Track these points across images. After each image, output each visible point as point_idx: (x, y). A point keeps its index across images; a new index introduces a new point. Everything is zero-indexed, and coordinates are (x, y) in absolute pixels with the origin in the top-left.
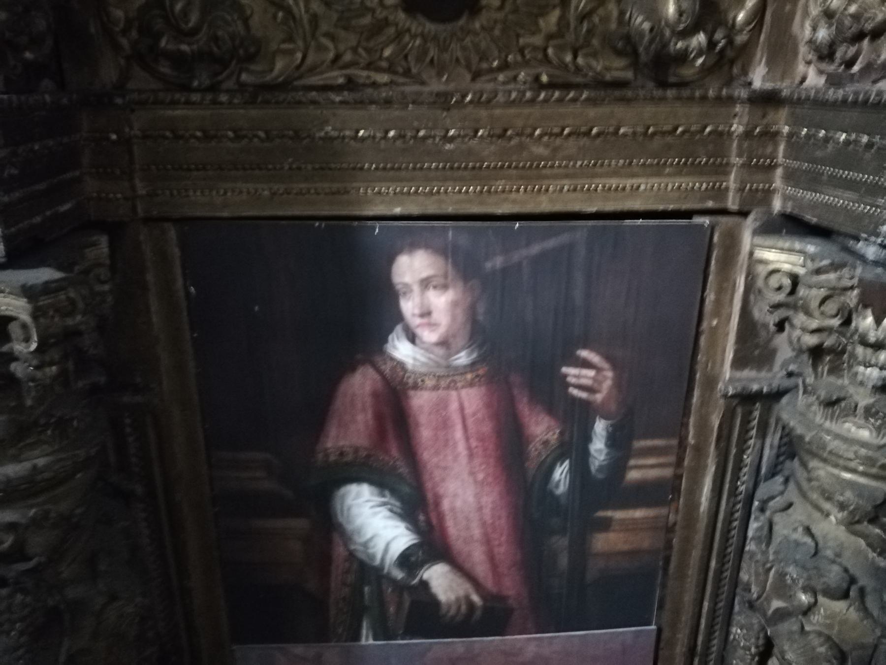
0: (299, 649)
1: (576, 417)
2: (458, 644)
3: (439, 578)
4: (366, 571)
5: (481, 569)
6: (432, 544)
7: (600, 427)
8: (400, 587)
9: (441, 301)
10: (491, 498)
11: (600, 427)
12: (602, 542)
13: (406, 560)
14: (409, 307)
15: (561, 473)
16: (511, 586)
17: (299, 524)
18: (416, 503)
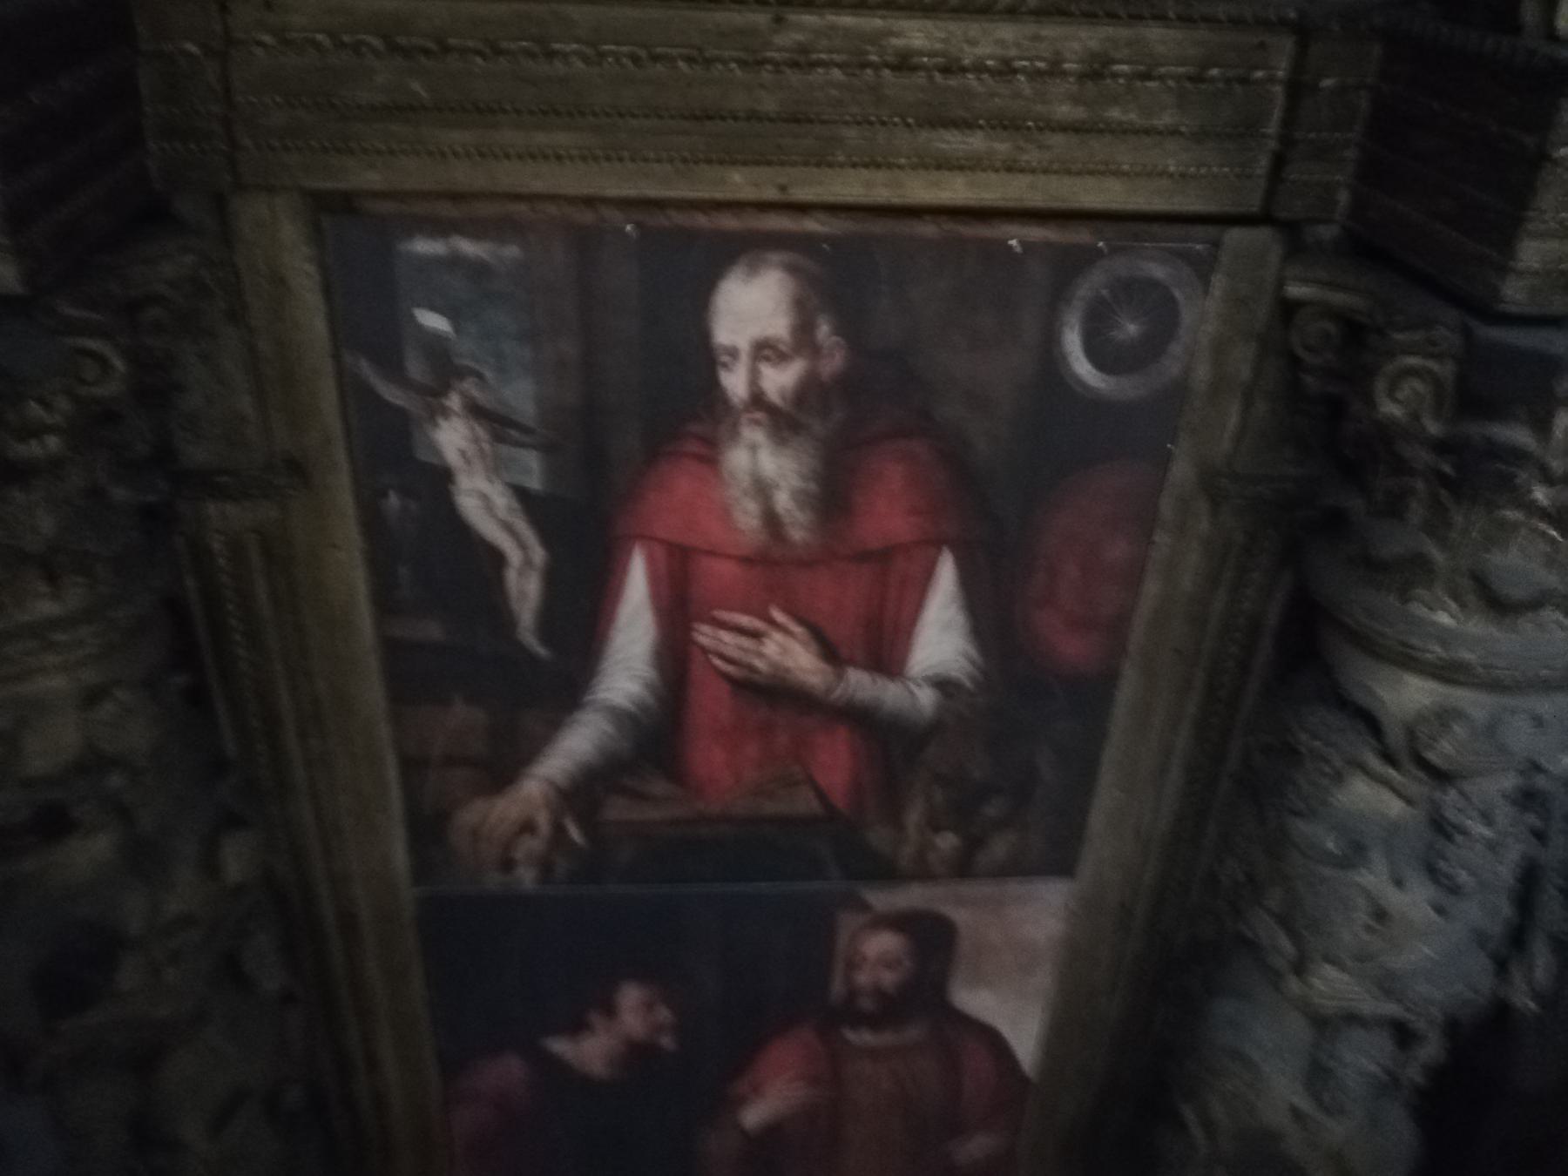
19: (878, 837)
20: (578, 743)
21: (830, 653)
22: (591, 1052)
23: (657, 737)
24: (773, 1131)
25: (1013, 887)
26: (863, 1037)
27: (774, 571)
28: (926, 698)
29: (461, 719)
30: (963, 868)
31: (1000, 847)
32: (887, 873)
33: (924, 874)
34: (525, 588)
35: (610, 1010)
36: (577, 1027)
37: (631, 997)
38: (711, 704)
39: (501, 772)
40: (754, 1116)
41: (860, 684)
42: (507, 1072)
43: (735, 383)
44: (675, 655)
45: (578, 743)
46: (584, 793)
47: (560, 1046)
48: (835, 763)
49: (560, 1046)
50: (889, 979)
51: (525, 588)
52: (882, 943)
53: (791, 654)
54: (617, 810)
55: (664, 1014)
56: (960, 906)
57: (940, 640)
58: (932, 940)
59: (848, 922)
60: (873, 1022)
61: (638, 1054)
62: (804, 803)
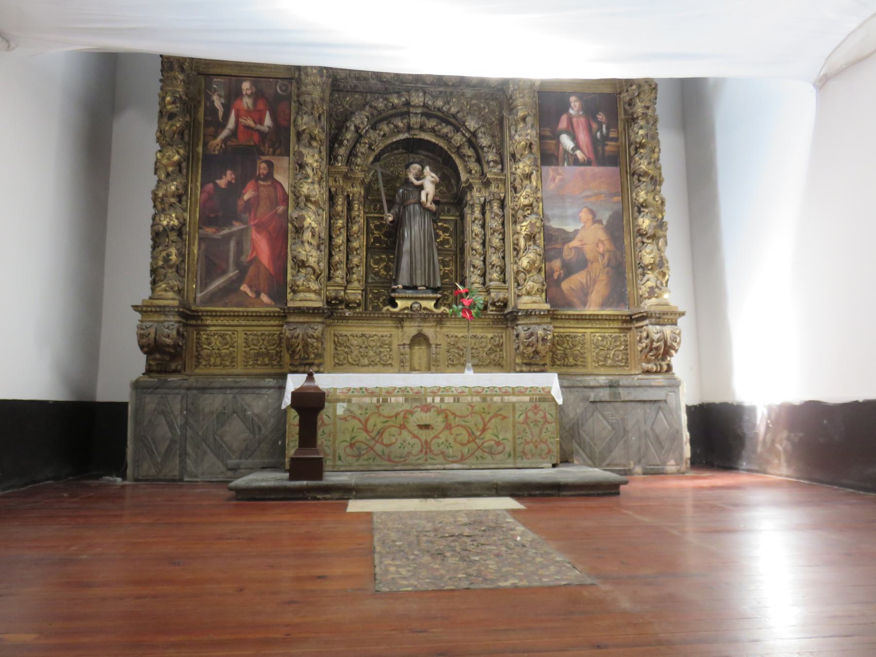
0: (553, 167)
1: (600, 124)
2: (583, 168)
3: (579, 153)
4: (566, 152)
5: (586, 152)
6: (577, 147)
7: (604, 126)
8: (572, 155)
9: (577, 104)
10: (587, 138)
11: (604, 126)
12: (607, 148)
13: (573, 149)
14: (572, 105)
15: (598, 134)
16: (592, 156)
17: (554, 142)
18: (574, 138)
19: (262, 149)
20: (225, 133)
21: (255, 123)
22: (222, 183)
23: (234, 133)
24: (249, 200)
25: (281, 158)
26: (261, 183)
27: (249, 113)
28: (267, 129)
29: (211, 130)
30: (274, 154)
31: (278, 151)
32: (263, 154)
33: (268, 154)
34: (221, 114)
35: (226, 175)
36: (221, 178)
37: (229, 172)
38: (241, 129)
39: (215, 136)
40: (246, 197)
41: (259, 127)
42: (210, 186)
43: (244, 92)
44: (237, 122)
45: (225, 133)
46: (225, 141)
47: (218, 181)
48: (256, 137)
49: (218, 181)
50: (265, 172)
51: (221, 114)
52: (263, 165)
53: (250, 122)
54: (229, 143)
55: (233, 176)
56: (274, 160)
57: (268, 121)
58: (270, 165)
59: (259, 162)
60: (264, 180)
61: (229, 183)
62: (252, 143)
